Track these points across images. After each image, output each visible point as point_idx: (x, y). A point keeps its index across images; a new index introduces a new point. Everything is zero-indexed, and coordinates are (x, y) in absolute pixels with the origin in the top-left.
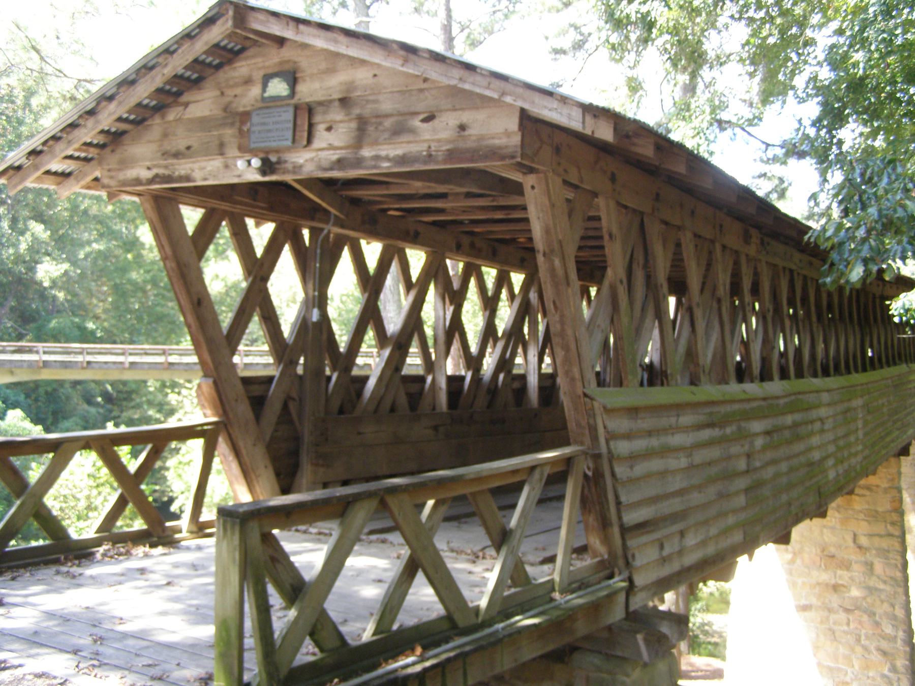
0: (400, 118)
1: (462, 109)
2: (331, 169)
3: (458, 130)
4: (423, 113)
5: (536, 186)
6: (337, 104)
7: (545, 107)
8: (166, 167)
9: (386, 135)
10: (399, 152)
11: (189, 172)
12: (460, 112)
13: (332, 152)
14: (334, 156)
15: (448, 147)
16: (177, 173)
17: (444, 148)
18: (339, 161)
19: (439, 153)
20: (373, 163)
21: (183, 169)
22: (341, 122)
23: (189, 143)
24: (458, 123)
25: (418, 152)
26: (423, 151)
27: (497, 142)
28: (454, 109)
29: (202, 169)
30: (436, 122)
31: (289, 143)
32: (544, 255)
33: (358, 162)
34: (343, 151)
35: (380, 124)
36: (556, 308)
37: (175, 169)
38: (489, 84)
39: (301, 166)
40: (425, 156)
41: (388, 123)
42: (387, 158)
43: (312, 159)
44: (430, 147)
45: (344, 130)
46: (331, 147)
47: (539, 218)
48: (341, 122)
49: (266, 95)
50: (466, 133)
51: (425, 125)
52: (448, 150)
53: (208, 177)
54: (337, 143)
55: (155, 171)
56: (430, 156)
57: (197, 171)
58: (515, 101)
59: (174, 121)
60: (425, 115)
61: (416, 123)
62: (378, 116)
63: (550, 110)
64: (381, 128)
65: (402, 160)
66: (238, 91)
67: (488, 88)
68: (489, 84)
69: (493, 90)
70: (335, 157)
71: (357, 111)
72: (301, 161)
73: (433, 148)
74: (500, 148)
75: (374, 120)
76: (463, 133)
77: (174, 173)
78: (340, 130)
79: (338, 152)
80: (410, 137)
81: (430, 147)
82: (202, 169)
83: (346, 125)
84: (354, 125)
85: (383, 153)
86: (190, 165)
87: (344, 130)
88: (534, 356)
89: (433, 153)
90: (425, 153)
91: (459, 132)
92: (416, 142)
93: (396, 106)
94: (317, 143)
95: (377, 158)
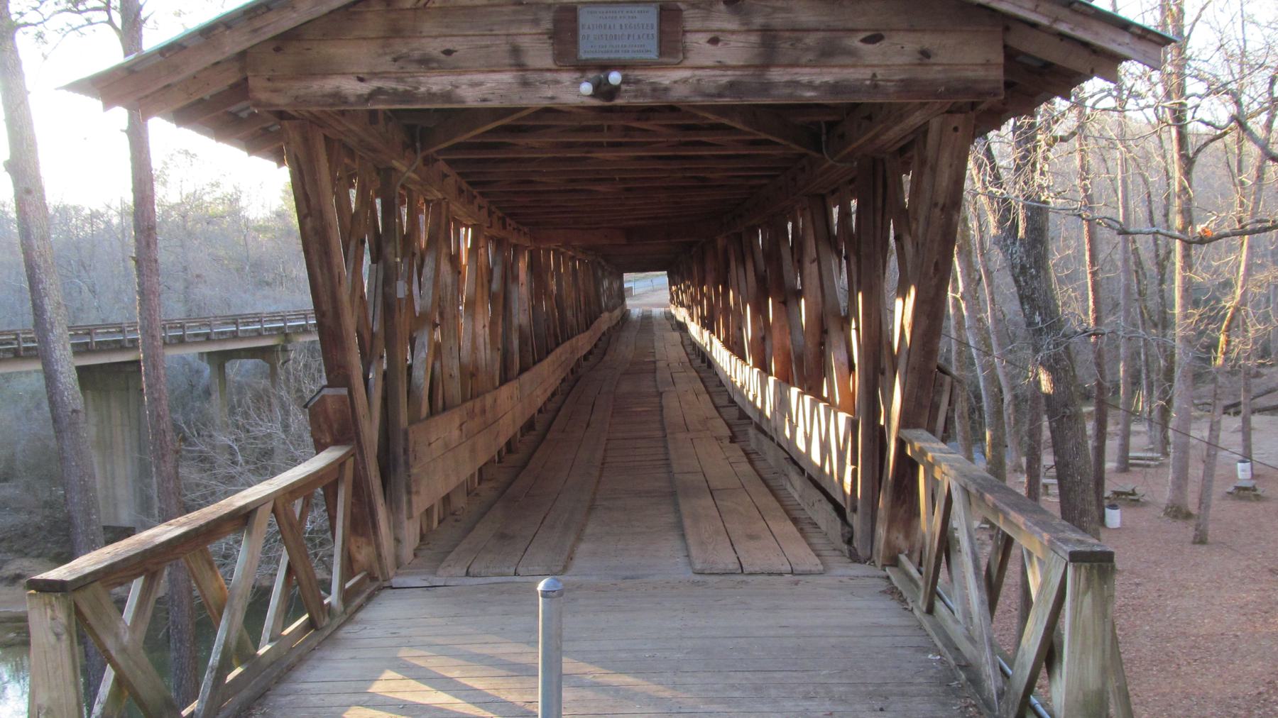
0: (828, 34)
1: (923, 31)
2: (720, 95)
3: (919, 56)
4: (865, 30)
5: (960, 129)
7: (1114, 41)
8: (400, 80)
9: (810, 56)
10: (829, 78)
12: (919, 35)
13: (718, 72)
14: (725, 78)
15: (902, 76)
16: (423, 89)
17: (897, 78)
18: (732, 85)
19: (889, 84)
20: (788, 91)
21: (435, 84)
22: (733, 32)
23: (449, 46)
24: (918, 47)
25: (857, 80)
26: (865, 80)
27: (970, 74)
28: (911, 30)
29: (474, 85)
30: (884, 43)
31: (653, 55)
32: (942, 209)
33: (767, 87)
34: (738, 73)
35: (799, 40)
36: (936, 269)
37: (420, 83)
38: (1037, 6)
39: (666, 89)
40: (867, 85)
41: (811, 39)
42: (810, 86)
43: (685, 81)
44: (874, 75)
45: (741, 45)
46: (722, 66)
47: (951, 166)
48: (733, 32)
50: (932, 60)
51: (870, 47)
52: (902, 80)
53: (490, 97)
55: (375, 84)
56: (876, 86)
57: (464, 87)
58: (1072, 29)
59: (411, 9)
60: (868, 34)
61: (855, 42)
62: (794, 30)
63: (1119, 45)
64: (800, 45)
65: (835, 88)
67: (1035, 11)
68: (1037, 6)
69: (1044, 15)
70: (724, 80)
71: (758, 21)
72: (666, 82)
73: (879, 77)
74: (975, 81)
75: (787, 34)
76: (927, 61)
77: (417, 88)
78: (732, 44)
79: (729, 73)
80: (848, 61)
81: (874, 75)
82: (474, 85)
83: (742, 37)
84: (754, 38)
85: (805, 79)
86: (452, 78)
87: (741, 45)
88: (484, 326)
89: (881, 83)
90: (868, 82)
91: (919, 59)
92: (854, 66)
93: (825, 19)
94: (694, 59)
95: (795, 84)
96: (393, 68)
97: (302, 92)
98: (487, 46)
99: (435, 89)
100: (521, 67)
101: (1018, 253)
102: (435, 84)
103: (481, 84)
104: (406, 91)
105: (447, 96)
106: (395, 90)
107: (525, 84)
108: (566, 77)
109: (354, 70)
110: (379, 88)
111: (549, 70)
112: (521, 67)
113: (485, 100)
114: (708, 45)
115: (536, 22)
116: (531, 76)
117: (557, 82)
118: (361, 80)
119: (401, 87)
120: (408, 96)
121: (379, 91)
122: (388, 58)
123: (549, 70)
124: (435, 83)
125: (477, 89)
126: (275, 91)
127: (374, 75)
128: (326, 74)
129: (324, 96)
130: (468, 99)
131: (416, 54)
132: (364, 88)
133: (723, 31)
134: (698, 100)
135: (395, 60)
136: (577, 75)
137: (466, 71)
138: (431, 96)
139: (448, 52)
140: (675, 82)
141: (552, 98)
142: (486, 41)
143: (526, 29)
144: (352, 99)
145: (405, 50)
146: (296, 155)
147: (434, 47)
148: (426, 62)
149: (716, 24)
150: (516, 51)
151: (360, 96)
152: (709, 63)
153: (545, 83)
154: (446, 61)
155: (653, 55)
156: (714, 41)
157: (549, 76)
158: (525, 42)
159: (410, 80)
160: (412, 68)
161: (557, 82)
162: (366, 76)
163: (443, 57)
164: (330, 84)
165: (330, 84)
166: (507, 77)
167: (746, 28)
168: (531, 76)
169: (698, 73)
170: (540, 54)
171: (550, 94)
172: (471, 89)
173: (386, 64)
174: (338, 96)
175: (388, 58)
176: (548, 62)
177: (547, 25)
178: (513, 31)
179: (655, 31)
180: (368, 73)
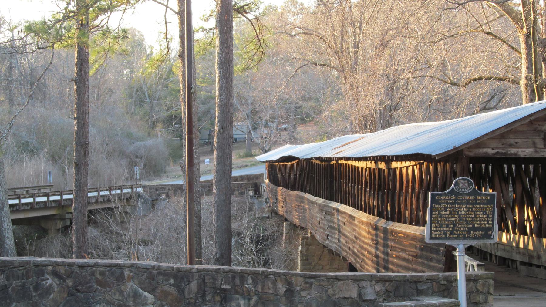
8: (503, 150)
16: (509, 152)
23: (517, 141)
29: (523, 151)
55: (497, 150)
66: (540, 123)
82: (523, 151)
86: (517, 150)
96: (502, 146)
97: (477, 152)
99: (513, 152)
100: (535, 147)
103: (524, 151)
105: (515, 154)
107: (536, 152)
109: (492, 147)
111: (542, 148)
112: (535, 147)
115: (539, 136)
116: (538, 150)
118: (493, 149)
119: (503, 152)
120: (505, 154)
121: (498, 152)
123: (542, 148)
124: (513, 151)
126: (470, 151)
127: (497, 148)
128: (484, 148)
131: (508, 143)
132: (494, 151)
135: (503, 145)
137: (521, 148)
138: (511, 154)
139: (516, 143)
141: (543, 155)
142: (526, 140)
143: (537, 138)
146: (464, 167)
147: (512, 141)
148: (511, 146)
150: (534, 143)
151: (493, 154)
154: (515, 145)
157: (542, 150)
163: (515, 144)
164: (485, 150)
165: (485, 150)
168: (538, 150)
171: (543, 154)
173: (500, 146)
174: (486, 153)
175: (501, 144)
176: (543, 146)
177: (542, 137)
178: (534, 138)
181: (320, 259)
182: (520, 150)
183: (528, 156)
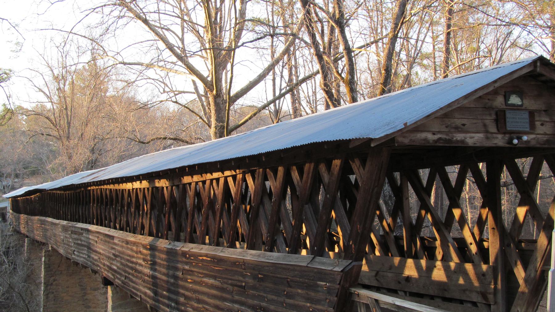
2: (544, 144)
6: (543, 113)
8: (447, 135)
11: (463, 138)
13: (544, 136)
14: (545, 138)
16: (455, 139)
21: (459, 137)
29: (471, 138)
31: (528, 130)
37: (454, 136)
43: (534, 139)
46: (545, 134)
48: (547, 122)
49: (509, 102)
53: (476, 142)
54: (548, 133)
55: (438, 136)
57: (468, 138)
70: (545, 139)
77: (453, 138)
78: (547, 126)
82: (471, 138)
96: (447, 130)
98: (476, 123)
99: (459, 139)
100: (487, 132)
101: (387, 190)
102: (459, 137)
103: (473, 137)
104: (449, 139)
105: (463, 141)
106: (445, 138)
107: (487, 138)
108: (500, 136)
109: (434, 130)
110: (440, 138)
111: (495, 133)
112: (487, 132)
113: (475, 144)
114: (541, 126)
115: (490, 115)
116: (489, 135)
117: (497, 138)
118: (434, 134)
119: (447, 138)
120: (450, 141)
121: (440, 139)
122: (444, 126)
123: (495, 133)
124: (459, 136)
125: (472, 139)
127: (439, 132)
129: (421, 140)
130: (469, 143)
131: (454, 125)
132: (436, 137)
133: (544, 121)
134: (538, 146)
136: (503, 135)
138: (457, 141)
139: (464, 125)
140: (532, 139)
141: (496, 144)
142: (475, 121)
143: (488, 118)
144: (431, 142)
145: (449, 123)
148: (458, 129)
149: (543, 119)
150: (485, 126)
151: (434, 140)
152: (542, 132)
153: (493, 138)
155: (528, 130)
156: (542, 125)
157: (495, 136)
158: (488, 122)
159: (450, 135)
160: (453, 130)
161: (497, 138)
162: (436, 133)
163: (462, 126)
164: (423, 135)
166: (481, 135)
167: (551, 120)
169: (538, 136)
170: (492, 128)
171: (495, 142)
172: (470, 140)
173: (444, 129)
174: (426, 140)
175: (444, 126)
177: (494, 117)
179: (528, 121)
180: (437, 132)
181: (59, 266)
182: (468, 135)
183: (478, 145)
